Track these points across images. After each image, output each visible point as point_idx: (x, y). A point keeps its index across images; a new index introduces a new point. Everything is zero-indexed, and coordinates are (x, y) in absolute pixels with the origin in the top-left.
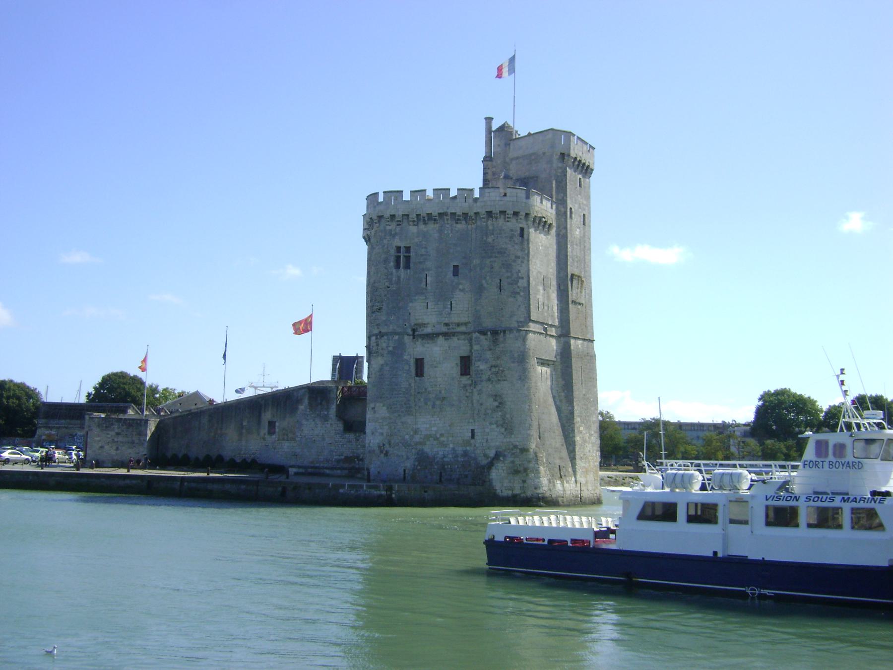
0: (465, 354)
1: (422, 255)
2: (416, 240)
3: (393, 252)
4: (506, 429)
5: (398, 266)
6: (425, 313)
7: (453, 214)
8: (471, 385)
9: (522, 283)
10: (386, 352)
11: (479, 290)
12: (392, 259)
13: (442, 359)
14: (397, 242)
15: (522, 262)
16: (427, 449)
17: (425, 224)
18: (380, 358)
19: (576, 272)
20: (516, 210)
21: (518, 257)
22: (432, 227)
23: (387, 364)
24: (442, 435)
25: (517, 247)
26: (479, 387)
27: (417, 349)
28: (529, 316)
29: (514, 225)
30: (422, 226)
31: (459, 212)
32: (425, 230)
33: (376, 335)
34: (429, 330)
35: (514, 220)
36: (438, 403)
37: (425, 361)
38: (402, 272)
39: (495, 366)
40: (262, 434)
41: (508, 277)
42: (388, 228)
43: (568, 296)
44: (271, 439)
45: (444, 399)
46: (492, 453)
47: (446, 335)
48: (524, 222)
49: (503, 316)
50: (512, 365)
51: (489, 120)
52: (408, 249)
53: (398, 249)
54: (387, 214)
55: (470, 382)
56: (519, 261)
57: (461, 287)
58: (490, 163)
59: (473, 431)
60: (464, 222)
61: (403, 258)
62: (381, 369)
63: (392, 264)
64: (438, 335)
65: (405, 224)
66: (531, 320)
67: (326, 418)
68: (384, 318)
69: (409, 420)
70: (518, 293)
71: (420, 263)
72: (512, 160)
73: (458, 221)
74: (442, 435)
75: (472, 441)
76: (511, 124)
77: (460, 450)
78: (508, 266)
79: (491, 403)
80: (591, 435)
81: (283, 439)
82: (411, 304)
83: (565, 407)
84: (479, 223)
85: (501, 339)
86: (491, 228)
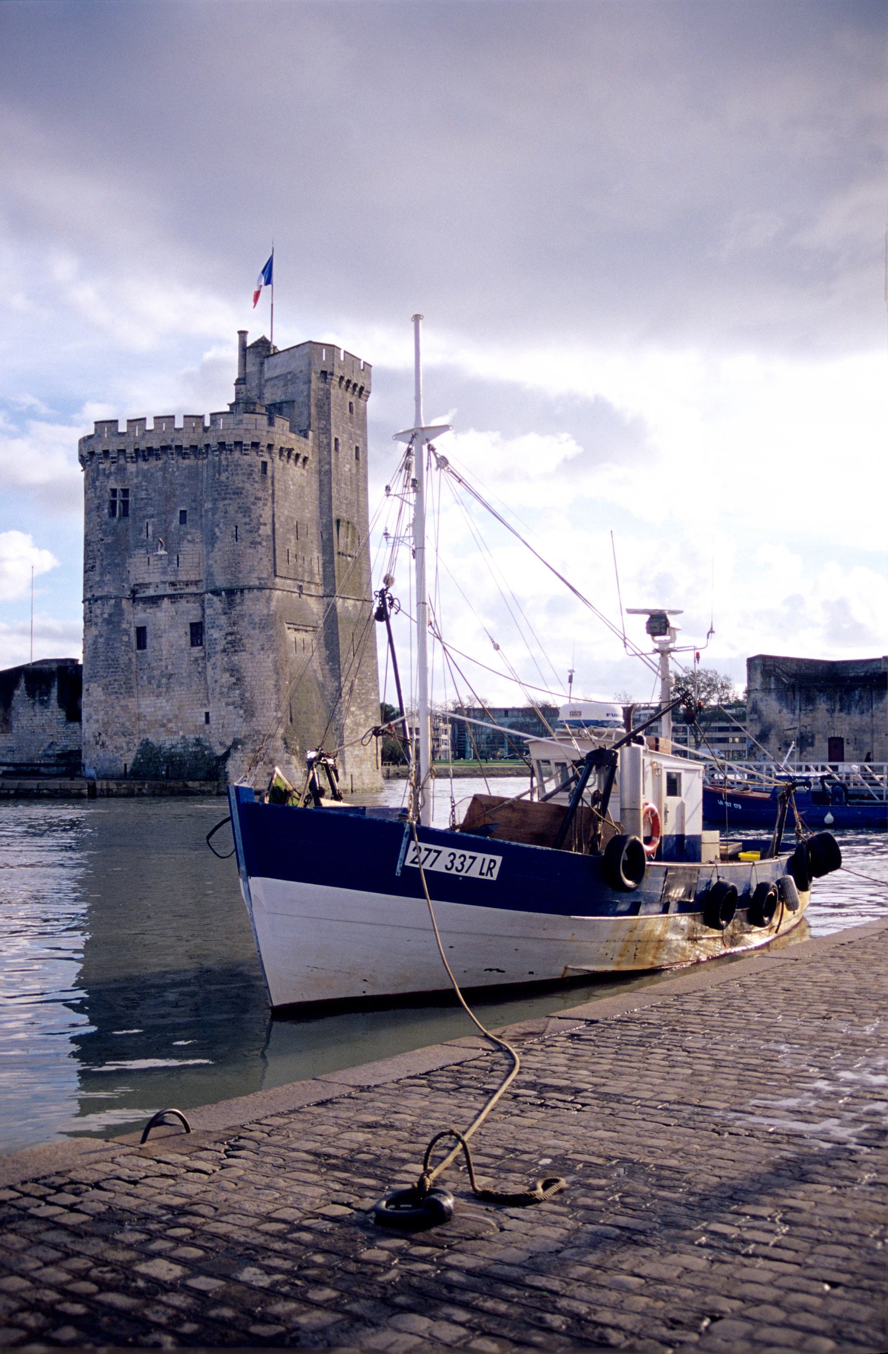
0: (196, 620)
2: (135, 481)
3: (107, 496)
4: (245, 711)
5: (113, 514)
7: (179, 448)
8: (203, 658)
9: (266, 530)
10: (100, 620)
11: (211, 540)
13: (168, 625)
14: (112, 484)
15: (265, 505)
16: (152, 739)
17: (145, 460)
18: (93, 628)
19: (344, 515)
20: (256, 440)
21: (260, 499)
23: (101, 636)
24: (170, 721)
25: (256, 486)
26: (213, 660)
27: (137, 615)
28: (275, 571)
29: (254, 459)
31: (185, 444)
32: (146, 467)
33: (89, 600)
34: (151, 592)
35: (253, 453)
36: (164, 681)
37: (148, 630)
39: (231, 634)
41: (246, 524)
43: (332, 547)
45: (170, 676)
48: (267, 455)
49: (240, 572)
50: (252, 632)
51: (243, 334)
52: (126, 492)
53: (114, 491)
54: (99, 449)
55: (202, 654)
56: (261, 503)
57: (189, 537)
58: (243, 386)
59: (207, 714)
60: (192, 457)
62: (95, 642)
63: (106, 511)
64: (161, 597)
65: (122, 462)
66: (276, 576)
67: (44, 704)
68: (97, 579)
69: (131, 703)
70: (260, 543)
71: (140, 509)
72: (267, 381)
73: (185, 456)
75: (207, 727)
76: (269, 339)
77: (191, 738)
78: (246, 511)
79: (226, 679)
80: (367, 717)
82: (129, 561)
83: (331, 685)
85: (238, 601)
86: (224, 463)
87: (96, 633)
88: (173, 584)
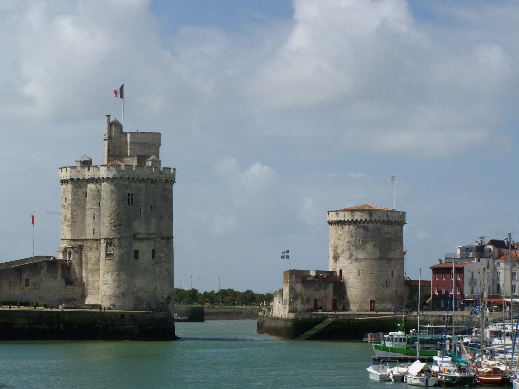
1: (139, 199)
5: (129, 204)
6: (139, 227)
12: (127, 199)
14: (129, 191)
16: (139, 294)
22: (143, 185)
26: (159, 265)
27: (137, 245)
30: (138, 184)
34: (141, 236)
36: (145, 272)
37: (139, 251)
38: (131, 207)
39: (168, 255)
40: (22, 286)
42: (125, 183)
44: (26, 289)
46: (166, 296)
47: (148, 239)
52: (132, 194)
53: (129, 194)
54: (126, 177)
61: (130, 199)
64: (145, 239)
74: (146, 288)
79: (166, 273)
81: (34, 289)
84: (160, 184)
87: (123, 252)
88: (148, 234)
